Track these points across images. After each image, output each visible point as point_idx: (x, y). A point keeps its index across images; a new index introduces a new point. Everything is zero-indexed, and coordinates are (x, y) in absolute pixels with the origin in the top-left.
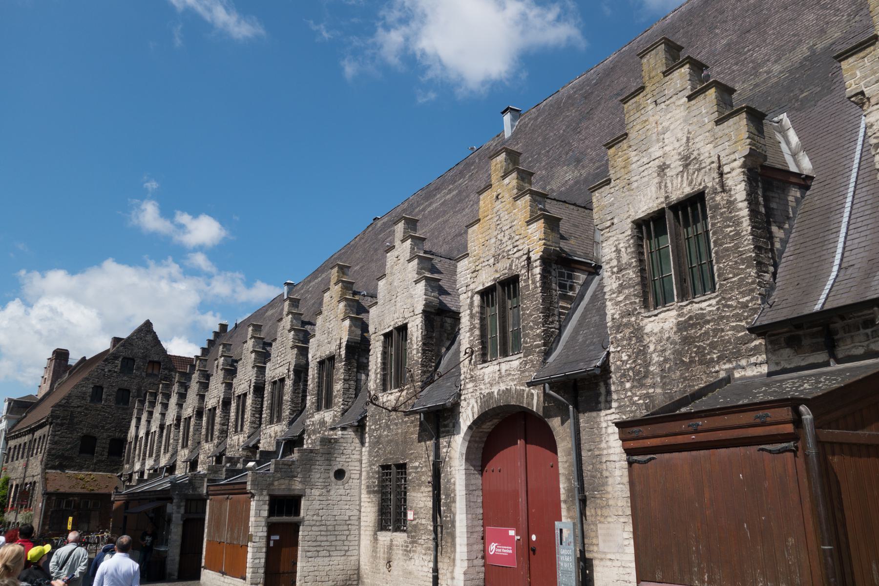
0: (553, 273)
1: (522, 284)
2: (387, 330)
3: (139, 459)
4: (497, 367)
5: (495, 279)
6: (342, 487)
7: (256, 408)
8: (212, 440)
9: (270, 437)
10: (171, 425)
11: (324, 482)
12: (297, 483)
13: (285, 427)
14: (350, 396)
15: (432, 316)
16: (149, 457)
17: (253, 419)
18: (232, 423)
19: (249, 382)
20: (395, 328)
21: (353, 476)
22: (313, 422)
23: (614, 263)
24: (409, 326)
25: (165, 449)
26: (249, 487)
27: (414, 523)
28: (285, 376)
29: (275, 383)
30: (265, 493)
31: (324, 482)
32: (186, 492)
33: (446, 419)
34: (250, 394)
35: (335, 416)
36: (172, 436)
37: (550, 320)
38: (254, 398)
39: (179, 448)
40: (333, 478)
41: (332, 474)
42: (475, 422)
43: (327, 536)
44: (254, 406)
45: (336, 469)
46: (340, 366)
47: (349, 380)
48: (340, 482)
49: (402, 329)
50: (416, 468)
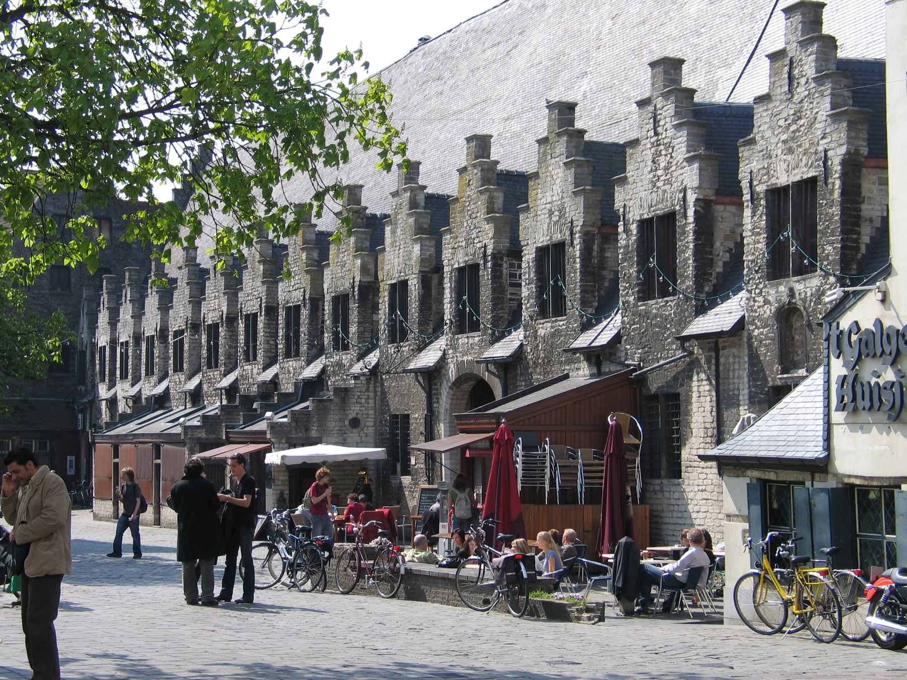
0: (505, 266)
1: (481, 273)
2: (393, 281)
3: (103, 380)
4: (466, 340)
5: (466, 262)
6: (357, 435)
7: (270, 333)
8: (216, 366)
9: (289, 372)
10: (153, 337)
11: (340, 430)
12: (314, 432)
13: (303, 363)
14: (366, 339)
15: (429, 275)
16: (121, 378)
17: (267, 346)
18: (242, 348)
19: (259, 300)
20: (399, 282)
21: (367, 424)
22: (332, 362)
23: (527, 276)
24: (409, 283)
25: (147, 370)
26: (268, 436)
27: (416, 467)
28: (300, 303)
29: (288, 309)
30: (284, 441)
31: (340, 430)
32: (199, 436)
33: (436, 378)
34: (261, 315)
35: (351, 359)
36: (156, 353)
37: (499, 306)
38: (266, 322)
39: (171, 372)
40: (348, 427)
41: (347, 423)
42: (453, 384)
43: (345, 479)
44: (268, 330)
45: (351, 417)
46: (354, 306)
47: (363, 323)
48: (355, 430)
49: (404, 284)
50: (416, 419)
